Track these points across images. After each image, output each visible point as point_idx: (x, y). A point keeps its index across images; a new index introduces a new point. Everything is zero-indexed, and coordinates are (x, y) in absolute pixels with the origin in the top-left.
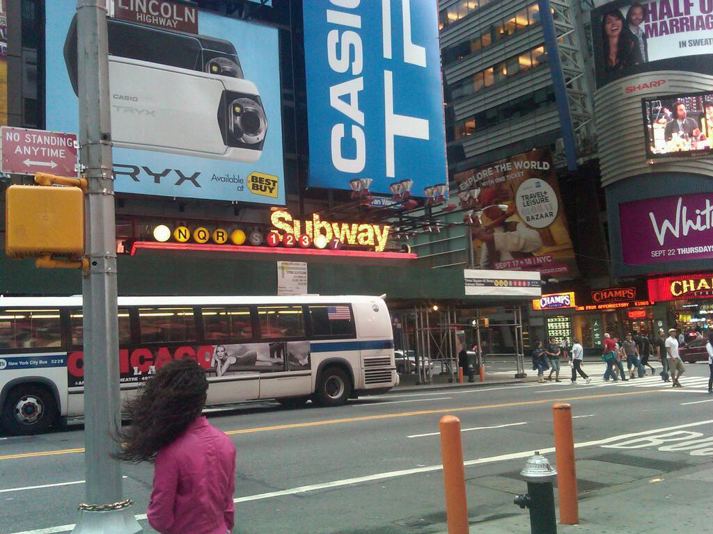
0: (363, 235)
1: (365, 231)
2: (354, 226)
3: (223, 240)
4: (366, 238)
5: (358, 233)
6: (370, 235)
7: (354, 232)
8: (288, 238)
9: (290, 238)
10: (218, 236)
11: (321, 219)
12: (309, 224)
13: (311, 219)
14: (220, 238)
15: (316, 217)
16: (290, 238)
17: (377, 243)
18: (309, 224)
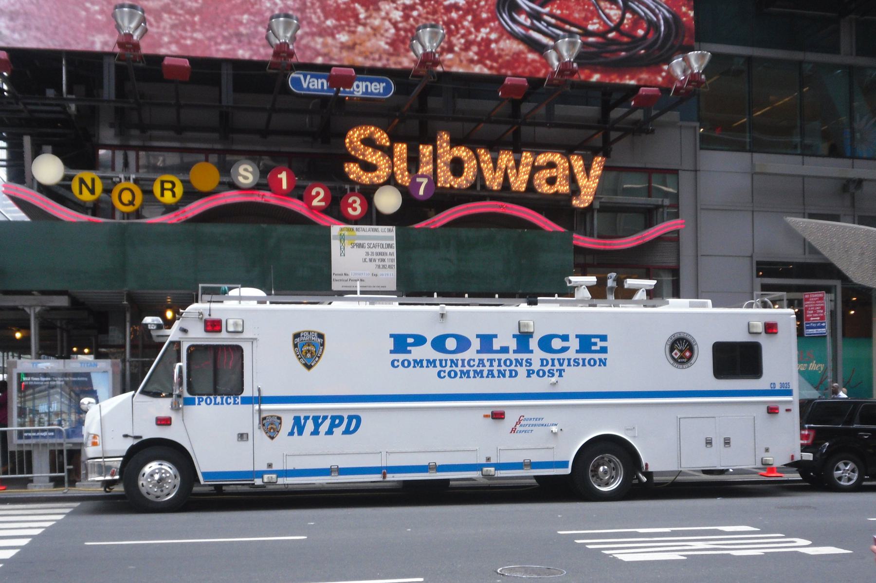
0: (546, 173)
1: (551, 165)
2: (527, 157)
3: (174, 195)
4: (551, 181)
5: (535, 169)
6: (560, 172)
8: (314, 193)
10: (163, 189)
11: (454, 142)
12: (426, 150)
13: (432, 141)
14: (168, 194)
16: (318, 194)
17: (576, 191)
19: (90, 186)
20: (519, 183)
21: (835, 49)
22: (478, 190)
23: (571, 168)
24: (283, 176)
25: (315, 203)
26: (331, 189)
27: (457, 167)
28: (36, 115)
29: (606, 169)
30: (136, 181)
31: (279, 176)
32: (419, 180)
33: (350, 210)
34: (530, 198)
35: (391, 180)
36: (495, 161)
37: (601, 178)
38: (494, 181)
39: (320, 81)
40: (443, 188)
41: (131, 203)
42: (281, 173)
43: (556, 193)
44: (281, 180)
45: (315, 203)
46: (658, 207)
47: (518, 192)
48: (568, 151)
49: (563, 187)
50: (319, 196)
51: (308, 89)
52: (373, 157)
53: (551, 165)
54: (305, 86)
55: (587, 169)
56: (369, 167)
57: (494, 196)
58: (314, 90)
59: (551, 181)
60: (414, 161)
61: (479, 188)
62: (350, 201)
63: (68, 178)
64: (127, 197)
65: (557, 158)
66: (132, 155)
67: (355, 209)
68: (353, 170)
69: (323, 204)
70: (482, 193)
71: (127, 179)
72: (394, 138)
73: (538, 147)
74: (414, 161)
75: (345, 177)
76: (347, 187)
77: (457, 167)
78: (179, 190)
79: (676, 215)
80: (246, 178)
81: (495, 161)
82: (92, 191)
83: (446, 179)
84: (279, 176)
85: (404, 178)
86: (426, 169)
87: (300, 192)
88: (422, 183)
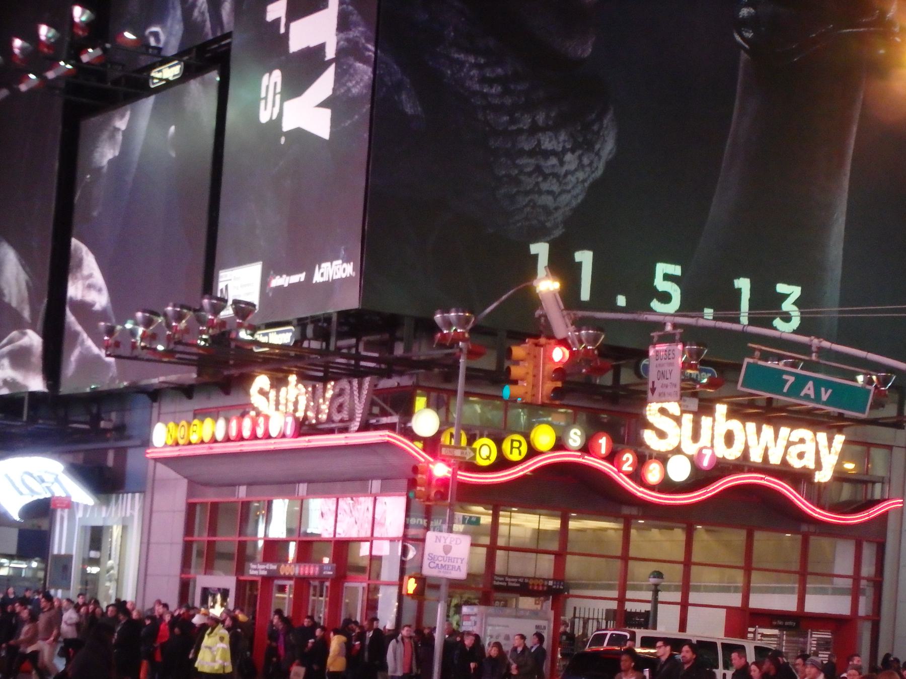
4: (801, 456)
5: (790, 444)
6: (809, 449)
7: (782, 442)
8: (624, 458)
9: (628, 459)
10: (512, 447)
12: (706, 421)
14: (516, 451)
16: (628, 459)
17: (819, 465)
27: (729, 439)
43: (804, 468)
50: (628, 459)
53: (802, 441)
56: (662, 435)
59: (801, 456)
68: (649, 437)
77: (729, 439)
78: (524, 449)
80: (575, 441)
87: (612, 457)
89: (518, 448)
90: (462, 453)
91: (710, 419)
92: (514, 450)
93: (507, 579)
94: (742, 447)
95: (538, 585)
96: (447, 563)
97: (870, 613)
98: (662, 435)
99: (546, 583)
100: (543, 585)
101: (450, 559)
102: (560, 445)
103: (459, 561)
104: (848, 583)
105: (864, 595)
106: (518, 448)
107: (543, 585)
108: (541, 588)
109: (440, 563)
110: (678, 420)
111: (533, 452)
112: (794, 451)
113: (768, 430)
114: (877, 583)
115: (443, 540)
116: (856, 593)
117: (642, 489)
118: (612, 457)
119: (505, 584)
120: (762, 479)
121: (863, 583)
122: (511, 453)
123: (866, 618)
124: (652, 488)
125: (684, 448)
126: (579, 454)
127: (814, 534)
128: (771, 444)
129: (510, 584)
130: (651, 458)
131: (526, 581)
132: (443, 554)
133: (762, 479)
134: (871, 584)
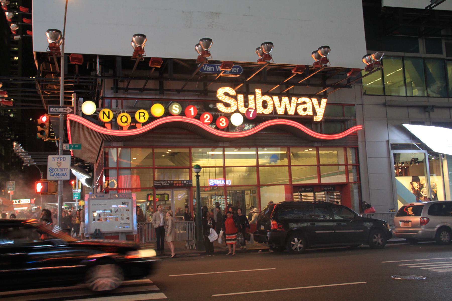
1: (304, 103)
3: (145, 119)
4: (305, 110)
5: (298, 105)
6: (309, 106)
7: (294, 104)
8: (205, 117)
9: (207, 117)
10: (140, 116)
11: (263, 94)
12: (251, 97)
13: (254, 93)
14: (142, 118)
15: (258, 91)
16: (207, 117)
17: (315, 113)
18: (251, 97)
19: (108, 115)
20: (291, 112)
21: (418, 52)
22: (274, 115)
23: (313, 104)
24: (192, 109)
25: (206, 121)
26: (212, 115)
27: (265, 105)
28: (82, 84)
29: (327, 104)
30: (126, 112)
31: (190, 109)
32: (250, 110)
33: (221, 124)
34: (296, 118)
35: (237, 111)
36: (280, 101)
37: (326, 108)
38: (281, 111)
39: (211, 68)
40: (259, 114)
41: (126, 122)
42: (190, 108)
43: (307, 115)
44: (191, 111)
45: (206, 121)
46: (347, 120)
47: (291, 115)
48: (310, 96)
49: (310, 112)
50: (207, 117)
51: (206, 71)
52: (231, 101)
53: (304, 103)
54: (205, 70)
55: (320, 104)
56: (227, 105)
57: (281, 117)
58: (209, 71)
59: (305, 110)
60: (246, 102)
61: (274, 113)
62: (221, 120)
63: (98, 111)
64: (124, 119)
65: (306, 99)
66: (120, 101)
67: (223, 124)
68: (220, 107)
69: (209, 122)
70: (275, 116)
71: (123, 112)
72: (238, 92)
73: (298, 96)
74: (246, 102)
75: (217, 110)
76: (219, 114)
77: (265, 105)
78: (147, 116)
79: (356, 124)
80: (176, 110)
81: (280, 101)
82: (109, 118)
83: (260, 110)
84: (190, 109)
85: (243, 110)
86: (251, 104)
87: (198, 117)
88: (251, 112)
89: (143, 116)
90: (64, 110)
91: (253, 96)
92: (141, 117)
93: (161, 182)
94: (272, 108)
95: (179, 183)
96: (59, 172)
97: (356, 181)
98: (227, 105)
99: (182, 182)
100: (181, 183)
101: (61, 169)
102: (168, 113)
103: (66, 170)
104: (343, 168)
105: (351, 172)
106: (143, 116)
107: (181, 183)
108: (180, 185)
109: (56, 172)
110: (235, 98)
111: (152, 118)
112: (300, 108)
113: (285, 99)
114: (357, 166)
115: (56, 159)
116: (347, 172)
117: (218, 131)
118: (198, 117)
119: (161, 184)
120: (284, 121)
121: (350, 167)
122: (139, 119)
123: (354, 183)
124: (223, 130)
125: (240, 110)
126: (180, 117)
127: (321, 147)
128: (288, 106)
129: (163, 184)
130: (221, 115)
131: (172, 182)
132: (57, 167)
133: (284, 121)
134: (355, 167)
